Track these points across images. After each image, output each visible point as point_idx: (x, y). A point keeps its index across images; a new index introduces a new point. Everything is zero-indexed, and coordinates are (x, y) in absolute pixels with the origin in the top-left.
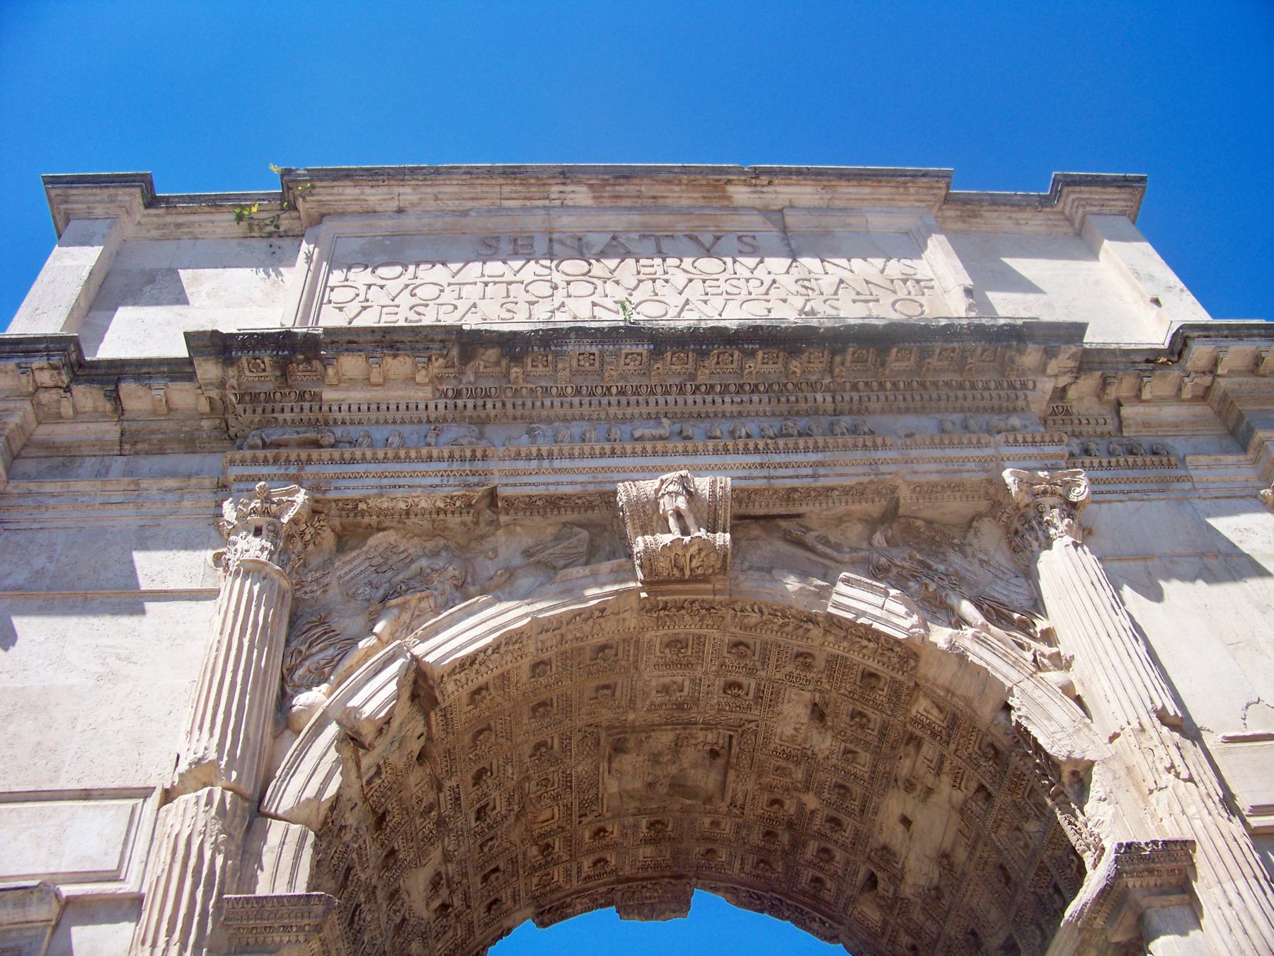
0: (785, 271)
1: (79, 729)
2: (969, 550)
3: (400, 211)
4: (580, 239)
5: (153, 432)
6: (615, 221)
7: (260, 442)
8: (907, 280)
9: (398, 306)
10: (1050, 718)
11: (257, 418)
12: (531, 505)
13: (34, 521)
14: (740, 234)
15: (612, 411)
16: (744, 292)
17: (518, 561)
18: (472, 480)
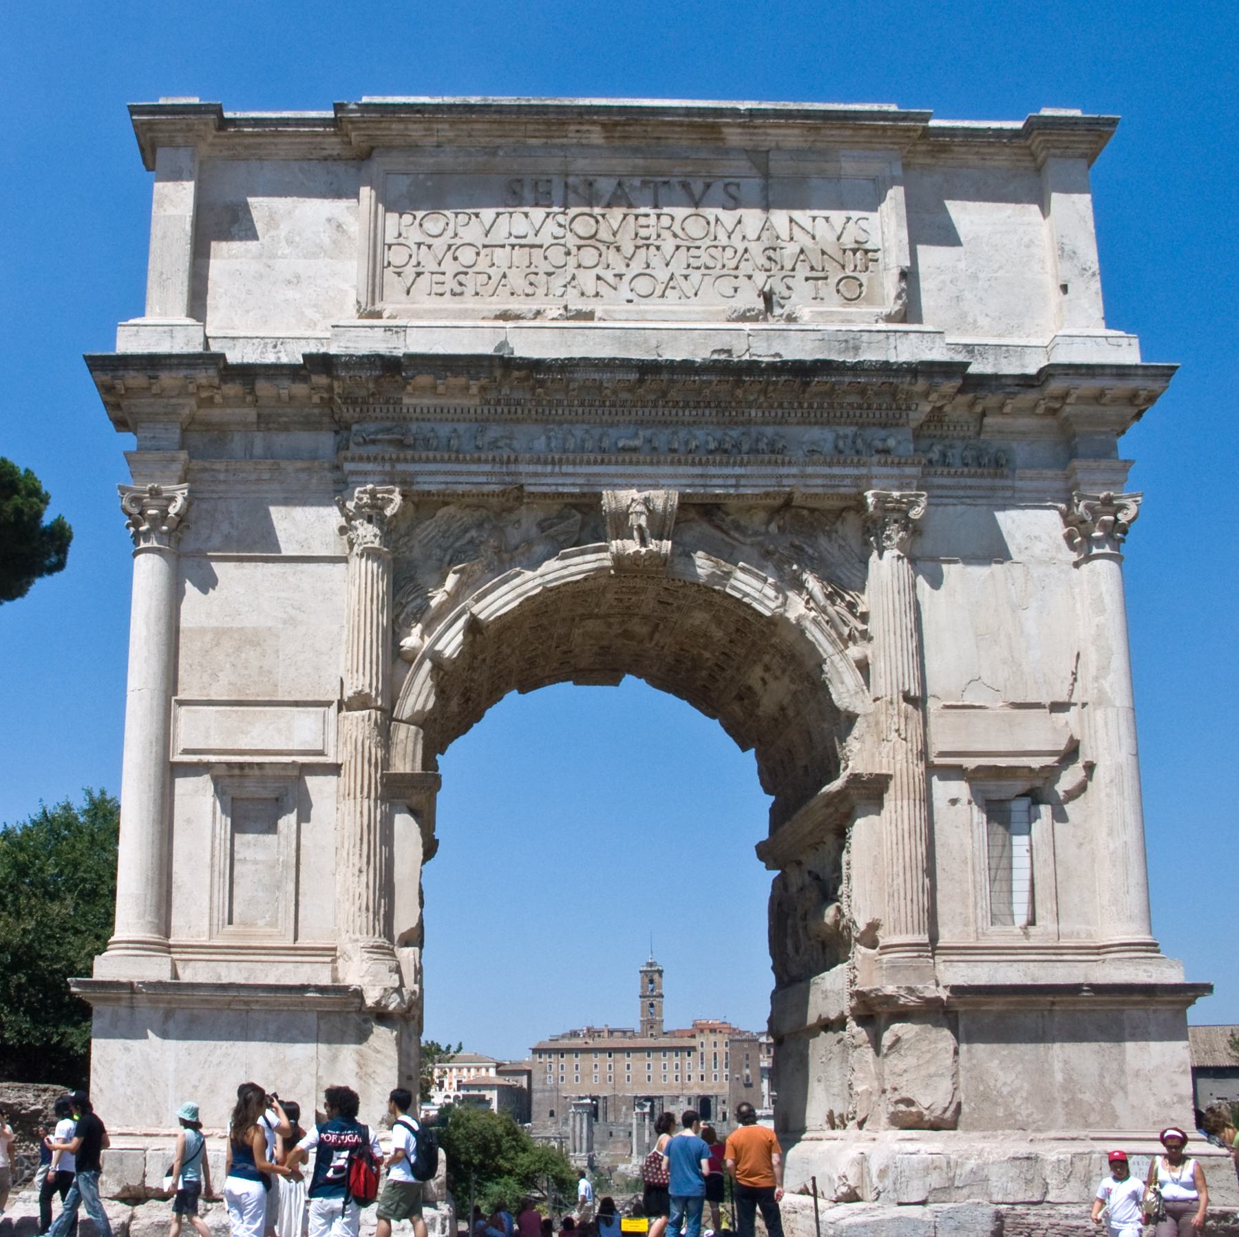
0: (756, 237)
1: (281, 658)
2: (834, 535)
3: (439, 146)
4: (591, 184)
5: (279, 416)
6: (620, 164)
7: (361, 440)
8: (858, 250)
9: (444, 274)
10: (842, 683)
11: (356, 415)
12: (545, 495)
13: (213, 492)
14: (727, 180)
15: (604, 418)
16: (719, 266)
17: (534, 531)
18: (508, 479)
